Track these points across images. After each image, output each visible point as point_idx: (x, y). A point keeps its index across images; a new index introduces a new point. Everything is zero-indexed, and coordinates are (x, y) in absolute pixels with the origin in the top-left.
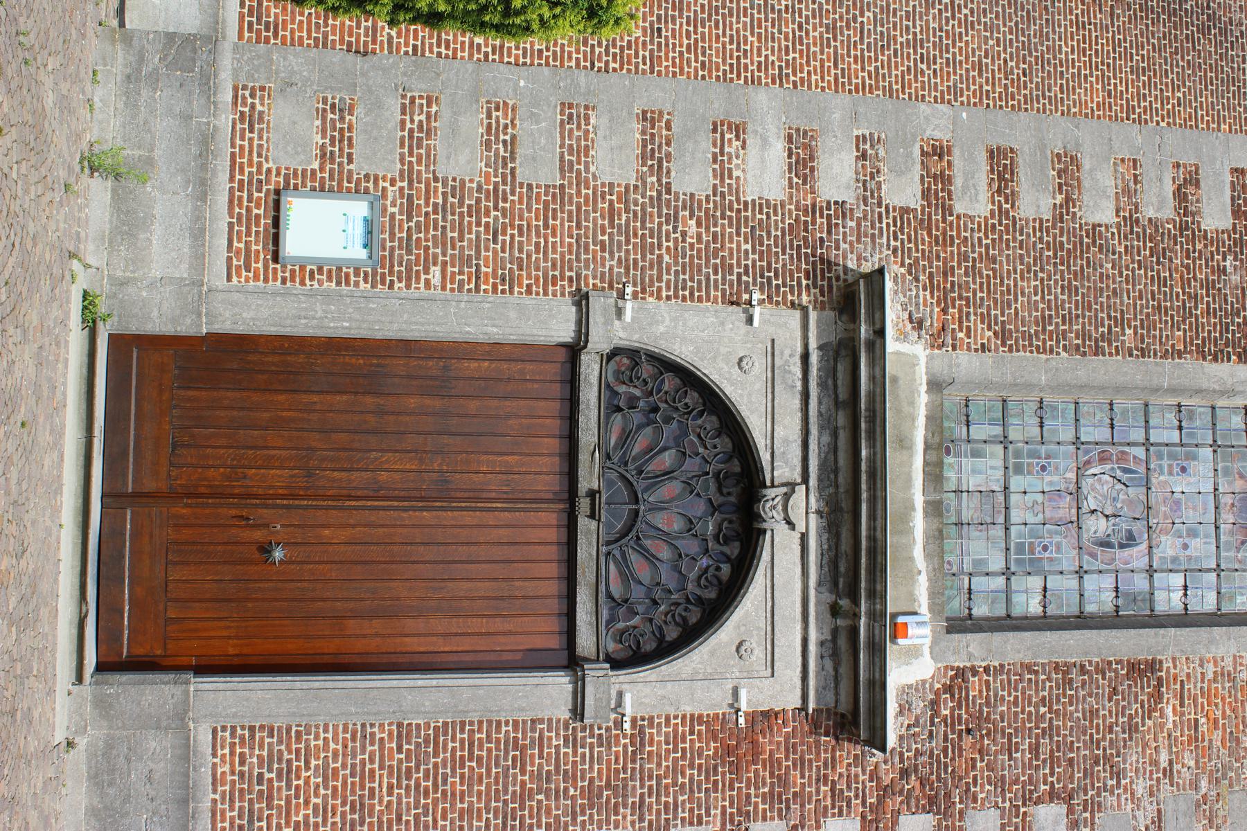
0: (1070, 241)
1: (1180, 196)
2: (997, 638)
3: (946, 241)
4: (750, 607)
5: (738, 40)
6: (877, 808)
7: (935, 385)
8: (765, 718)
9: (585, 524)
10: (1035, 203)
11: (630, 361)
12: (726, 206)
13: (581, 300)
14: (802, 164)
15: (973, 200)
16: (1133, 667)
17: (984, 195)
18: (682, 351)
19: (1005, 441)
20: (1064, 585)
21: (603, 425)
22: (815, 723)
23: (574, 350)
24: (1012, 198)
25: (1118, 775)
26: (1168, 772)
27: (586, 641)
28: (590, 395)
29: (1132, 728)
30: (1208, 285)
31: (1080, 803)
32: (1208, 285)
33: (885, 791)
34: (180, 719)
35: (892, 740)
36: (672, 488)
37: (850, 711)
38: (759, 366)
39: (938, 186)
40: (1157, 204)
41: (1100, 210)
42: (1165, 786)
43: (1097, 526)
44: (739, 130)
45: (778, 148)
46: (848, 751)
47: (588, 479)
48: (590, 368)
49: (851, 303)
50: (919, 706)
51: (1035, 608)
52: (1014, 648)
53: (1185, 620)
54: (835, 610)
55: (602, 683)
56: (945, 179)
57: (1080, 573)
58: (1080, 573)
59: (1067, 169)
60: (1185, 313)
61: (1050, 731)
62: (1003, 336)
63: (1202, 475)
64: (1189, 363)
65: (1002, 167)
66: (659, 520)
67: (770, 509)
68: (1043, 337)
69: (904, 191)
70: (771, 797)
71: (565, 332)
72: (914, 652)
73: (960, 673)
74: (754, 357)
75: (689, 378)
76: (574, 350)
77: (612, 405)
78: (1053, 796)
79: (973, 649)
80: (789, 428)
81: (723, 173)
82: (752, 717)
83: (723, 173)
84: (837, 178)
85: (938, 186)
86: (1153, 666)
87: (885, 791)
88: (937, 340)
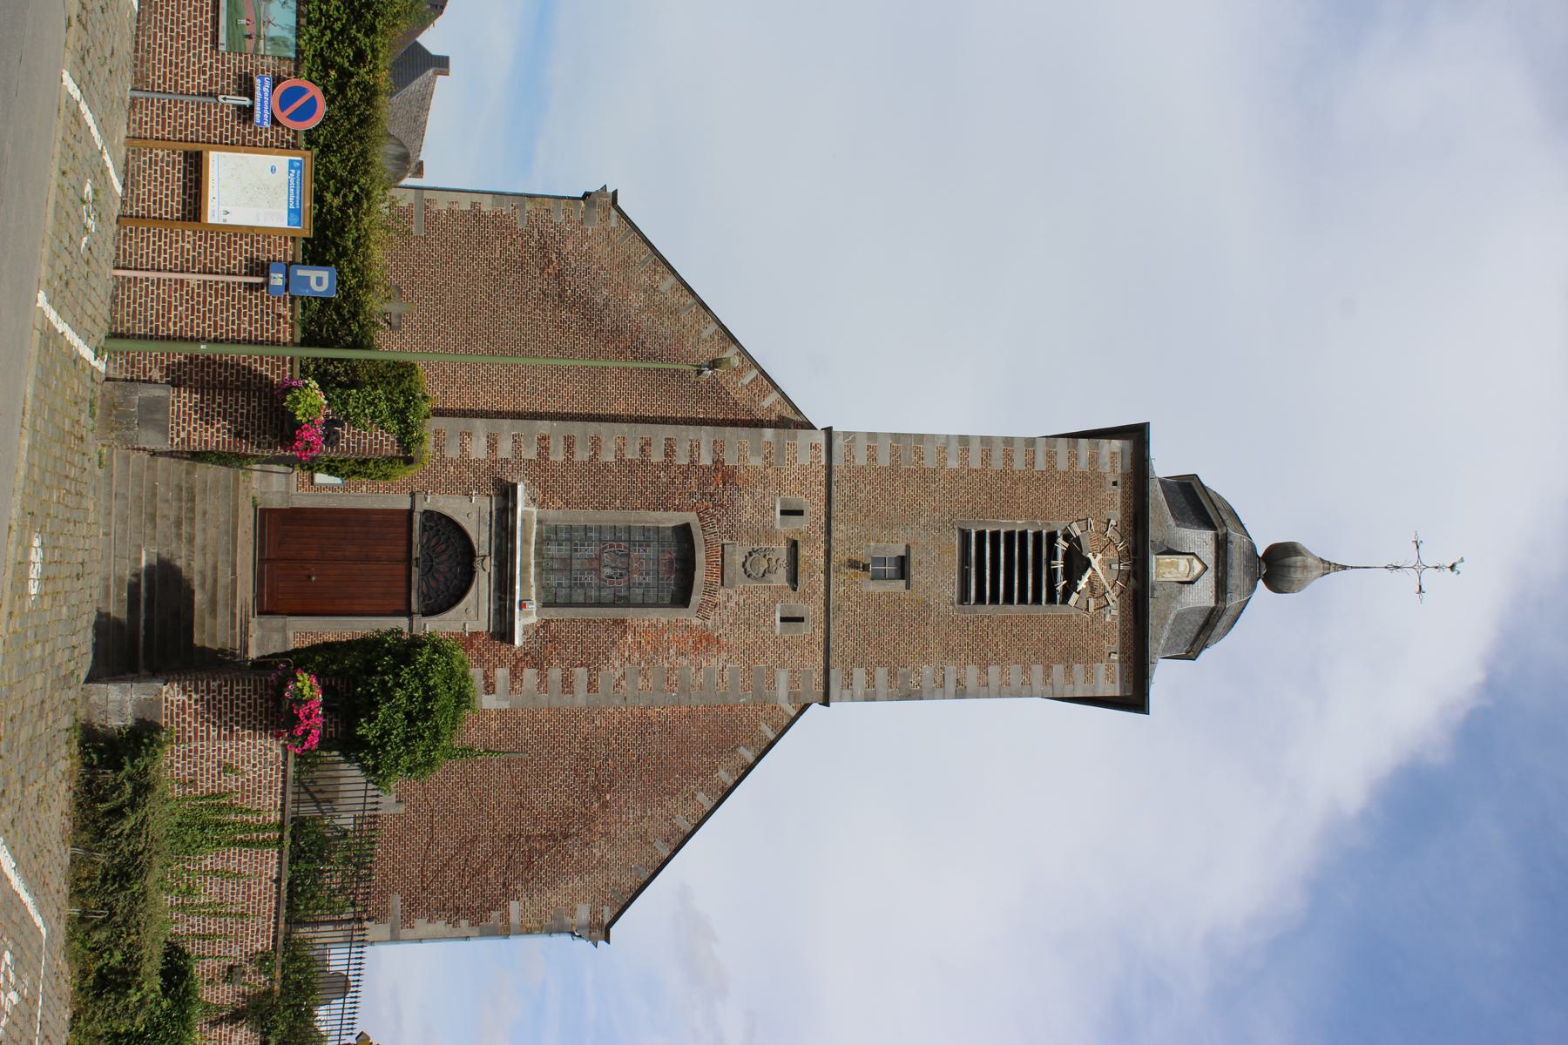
0: (597, 469)
1: (642, 450)
2: (561, 610)
3: (546, 470)
4: (470, 596)
5: (476, 394)
6: (516, 666)
7: (539, 522)
8: (475, 635)
9: (414, 569)
10: (582, 455)
11: (429, 515)
12: (464, 462)
13: (413, 495)
14: (492, 446)
15: (557, 455)
16: (615, 621)
17: (561, 452)
18: (448, 512)
19: (570, 540)
20: (593, 593)
21: (421, 536)
22: (493, 636)
23: (411, 512)
24: (573, 454)
25: (608, 659)
26: (629, 659)
27: (414, 607)
28: (417, 526)
29: (614, 643)
30: (652, 483)
31: (593, 666)
32: (652, 483)
33: (520, 660)
34: (284, 629)
35: (518, 642)
36: (444, 557)
37: (504, 633)
38: (474, 516)
39: (544, 450)
40: (632, 453)
41: (608, 457)
42: (627, 665)
43: (608, 571)
44: (469, 435)
45: (484, 440)
46: (505, 646)
47: (416, 553)
48: (417, 518)
49: (506, 493)
50: (531, 632)
51: (581, 599)
52: (568, 613)
53: (643, 605)
54: (500, 599)
55: (419, 621)
56: (547, 448)
57: (600, 588)
58: (600, 588)
59: (596, 443)
60: (641, 493)
61: (582, 642)
62: (567, 504)
63: (651, 552)
64: (642, 512)
65: (569, 443)
66: (441, 568)
67: (477, 565)
68: (583, 503)
69: (530, 453)
70: (477, 661)
71: (408, 506)
72: (530, 613)
73: (547, 621)
74: (472, 513)
75: (450, 521)
76: (411, 512)
77: (424, 528)
78: (582, 665)
79: (552, 613)
80: (485, 537)
81: (463, 450)
82: (471, 634)
83: (463, 450)
84: (505, 449)
85: (544, 450)
86: (623, 621)
87: (519, 660)
88: (541, 506)
